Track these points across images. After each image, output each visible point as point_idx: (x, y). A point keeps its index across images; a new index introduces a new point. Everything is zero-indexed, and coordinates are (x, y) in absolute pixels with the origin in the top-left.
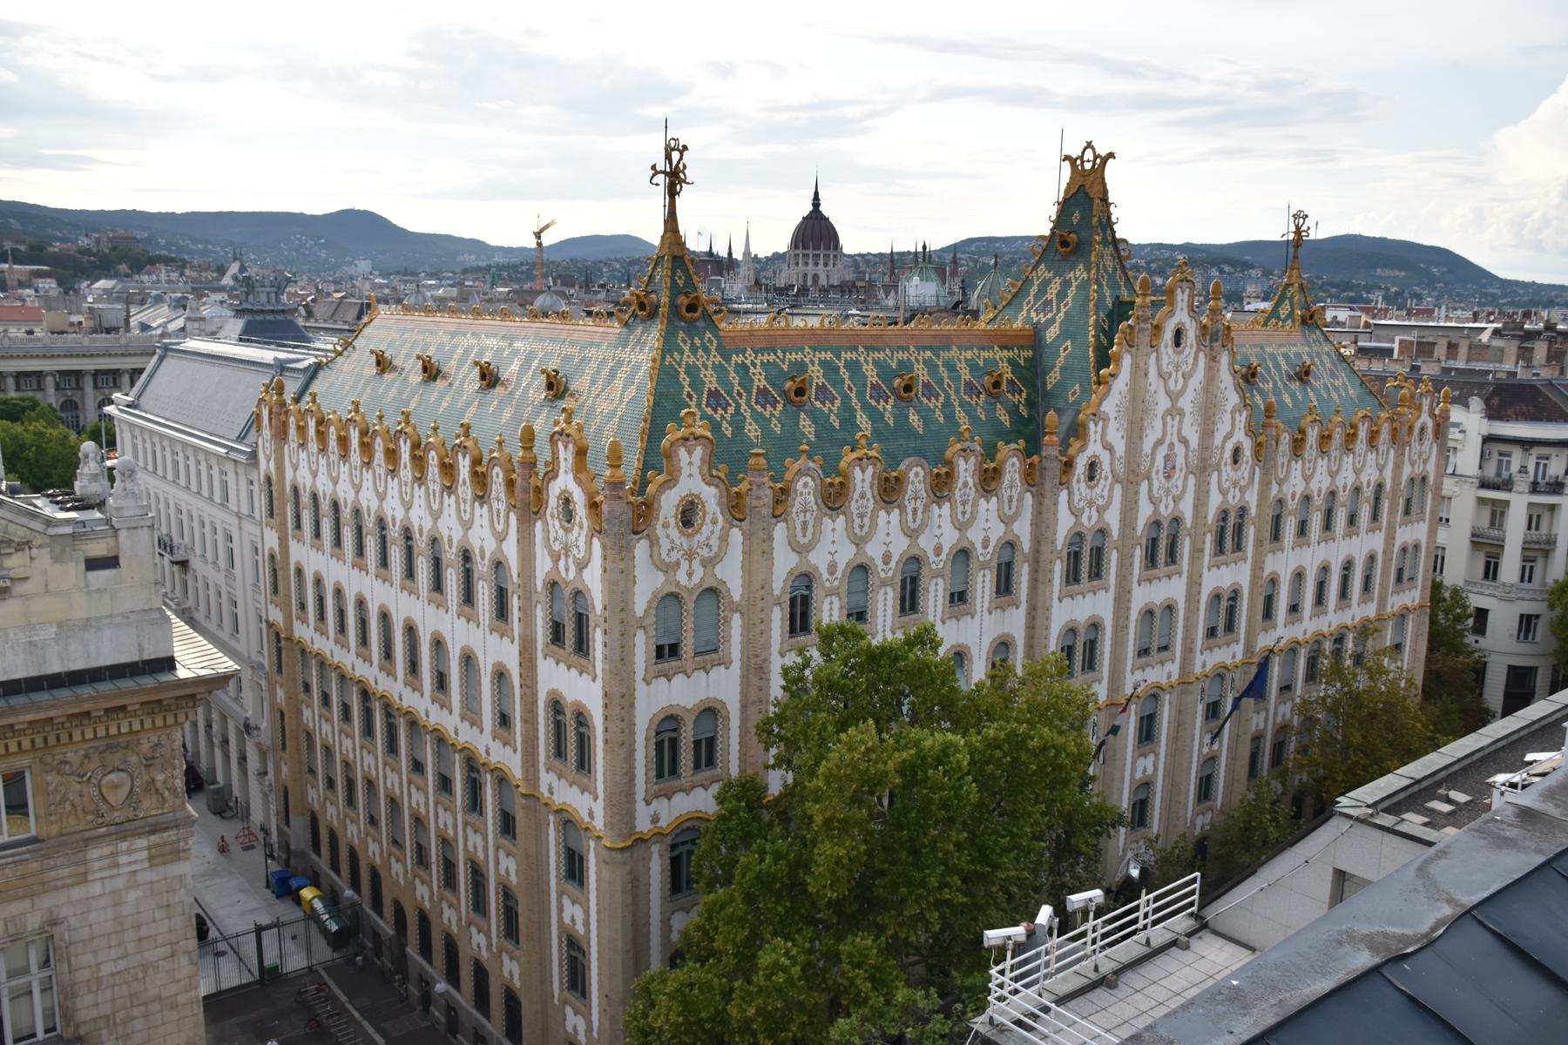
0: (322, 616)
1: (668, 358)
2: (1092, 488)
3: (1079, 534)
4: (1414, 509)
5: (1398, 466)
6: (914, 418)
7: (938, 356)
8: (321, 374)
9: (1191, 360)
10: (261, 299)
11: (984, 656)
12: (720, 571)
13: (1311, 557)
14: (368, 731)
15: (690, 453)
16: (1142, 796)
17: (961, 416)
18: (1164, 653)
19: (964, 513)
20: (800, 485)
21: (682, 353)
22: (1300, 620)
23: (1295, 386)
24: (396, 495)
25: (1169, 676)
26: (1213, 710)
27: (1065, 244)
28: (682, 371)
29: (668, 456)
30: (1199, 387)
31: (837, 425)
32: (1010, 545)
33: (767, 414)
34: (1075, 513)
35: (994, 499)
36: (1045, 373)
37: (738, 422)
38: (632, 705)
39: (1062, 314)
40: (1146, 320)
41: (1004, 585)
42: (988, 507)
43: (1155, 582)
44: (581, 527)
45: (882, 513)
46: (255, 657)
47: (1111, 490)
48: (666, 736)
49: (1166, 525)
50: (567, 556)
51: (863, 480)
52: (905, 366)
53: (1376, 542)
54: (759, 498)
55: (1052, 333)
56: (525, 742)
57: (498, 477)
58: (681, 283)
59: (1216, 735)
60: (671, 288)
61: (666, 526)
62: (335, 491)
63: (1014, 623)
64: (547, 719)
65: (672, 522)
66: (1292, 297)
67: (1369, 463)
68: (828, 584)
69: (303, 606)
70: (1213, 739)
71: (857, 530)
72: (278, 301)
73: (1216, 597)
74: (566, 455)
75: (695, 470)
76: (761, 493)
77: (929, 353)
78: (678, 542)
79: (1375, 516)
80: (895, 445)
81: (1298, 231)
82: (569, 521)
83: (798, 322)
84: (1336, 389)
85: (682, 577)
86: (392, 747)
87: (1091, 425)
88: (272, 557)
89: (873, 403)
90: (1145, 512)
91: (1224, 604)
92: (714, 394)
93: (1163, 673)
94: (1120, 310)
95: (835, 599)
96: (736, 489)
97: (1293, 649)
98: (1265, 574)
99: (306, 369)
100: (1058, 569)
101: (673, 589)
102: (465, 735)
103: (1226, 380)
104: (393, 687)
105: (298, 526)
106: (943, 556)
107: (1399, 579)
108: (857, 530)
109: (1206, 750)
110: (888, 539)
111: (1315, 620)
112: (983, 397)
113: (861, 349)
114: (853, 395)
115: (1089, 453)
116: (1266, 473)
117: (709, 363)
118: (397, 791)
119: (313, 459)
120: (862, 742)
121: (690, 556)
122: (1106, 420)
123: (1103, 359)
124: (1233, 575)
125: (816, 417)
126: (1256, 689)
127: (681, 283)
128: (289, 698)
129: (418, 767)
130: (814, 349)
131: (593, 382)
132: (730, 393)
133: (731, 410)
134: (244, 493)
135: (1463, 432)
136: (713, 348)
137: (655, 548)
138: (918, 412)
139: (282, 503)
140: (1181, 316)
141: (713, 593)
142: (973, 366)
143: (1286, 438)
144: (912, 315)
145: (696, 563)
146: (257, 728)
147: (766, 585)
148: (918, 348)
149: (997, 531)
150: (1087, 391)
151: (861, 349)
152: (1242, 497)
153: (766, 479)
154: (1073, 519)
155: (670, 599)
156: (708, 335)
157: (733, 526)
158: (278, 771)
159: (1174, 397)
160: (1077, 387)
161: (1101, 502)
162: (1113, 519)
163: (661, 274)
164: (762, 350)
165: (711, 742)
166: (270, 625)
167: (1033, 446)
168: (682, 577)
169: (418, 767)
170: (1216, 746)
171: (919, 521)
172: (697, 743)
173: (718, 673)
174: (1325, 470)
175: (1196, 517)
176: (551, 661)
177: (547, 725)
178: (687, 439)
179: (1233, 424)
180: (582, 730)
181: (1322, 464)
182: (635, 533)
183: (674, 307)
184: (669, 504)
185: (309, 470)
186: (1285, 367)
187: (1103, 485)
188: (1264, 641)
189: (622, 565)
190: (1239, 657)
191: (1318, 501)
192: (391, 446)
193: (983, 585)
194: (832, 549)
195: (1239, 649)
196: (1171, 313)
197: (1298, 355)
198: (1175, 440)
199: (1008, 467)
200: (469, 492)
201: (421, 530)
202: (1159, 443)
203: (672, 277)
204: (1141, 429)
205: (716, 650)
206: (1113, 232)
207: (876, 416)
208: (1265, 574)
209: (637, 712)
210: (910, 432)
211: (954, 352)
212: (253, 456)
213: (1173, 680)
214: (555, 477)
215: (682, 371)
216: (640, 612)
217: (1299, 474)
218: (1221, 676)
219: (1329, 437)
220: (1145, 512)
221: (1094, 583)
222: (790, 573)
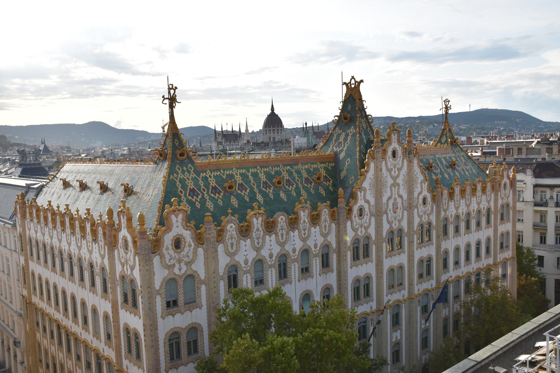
0: (42, 293)
1: (171, 176)
2: (361, 219)
3: (357, 239)
4: (505, 218)
5: (496, 200)
6: (282, 195)
7: (293, 168)
8: (45, 190)
9: (400, 163)
10: (31, 159)
11: (319, 294)
12: (194, 267)
13: (462, 241)
14: (60, 343)
15: (177, 217)
16: (397, 349)
17: (303, 192)
18: (401, 286)
19: (305, 234)
20: (228, 227)
21: (178, 174)
22: (460, 267)
23: (450, 170)
24: (65, 240)
25: (403, 296)
26: (425, 309)
27: (345, 118)
28: (178, 181)
29: (167, 219)
31: (248, 200)
32: (327, 246)
33: (216, 197)
34: (355, 230)
35: (318, 227)
36: (341, 171)
37: (203, 202)
38: (157, 329)
40: (378, 148)
41: (326, 264)
42: (316, 231)
43: (393, 257)
44: (131, 252)
45: (267, 237)
46: (19, 311)
47: (370, 219)
48: (174, 341)
49: (396, 232)
50: (127, 264)
51: (257, 223)
52: (278, 173)
53: (490, 232)
54: (209, 234)
55: (342, 155)
56: (116, 346)
57: (100, 230)
58: (177, 144)
59: (427, 320)
60: (175, 146)
61: (167, 249)
62: (44, 239)
63: (332, 279)
64: (124, 336)
65: (170, 247)
67: (483, 200)
68: (245, 269)
69: (35, 289)
70: (426, 321)
71: (256, 245)
72: (36, 160)
73: (421, 261)
74: (124, 221)
75: (179, 224)
76: (210, 232)
77: (288, 167)
78: (173, 255)
79: (488, 222)
80: (272, 208)
81: (447, 108)
82: (127, 249)
83: (252, 157)
84: (467, 170)
85: (176, 271)
86: (69, 350)
87: (359, 193)
88: (23, 268)
89: (264, 189)
90: (386, 227)
91: (425, 264)
92: (192, 191)
93: (401, 295)
94: (369, 144)
95: (248, 275)
96: (199, 231)
97: (458, 280)
98: (442, 249)
99: (37, 188)
100: (349, 255)
101: (173, 276)
102: (95, 344)
103: (417, 169)
104: (67, 322)
105: (32, 255)
106: (297, 253)
107: (502, 247)
108: (256, 245)
109: (423, 326)
110: (271, 247)
111: (466, 267)
112: (313, 184)
113: (258, 167)
114: (255, 187)
116: (438, 207)
117: (190, 177)
118: (72, 369)
119: (36, 226)
120: (243, 344)
121: (180, 261)
122: (365, 190)
123: (363, 166)
124: (429, 251)
125: (238, 197)
126: (443, 297)
127: (177, 144)
128: (30, 329)
129: (78, 358)
130: (237, 169)
131: (142, 188)
132: (199, 190)
133: (200, 197)
134: (12, 240)
135: (524, 184)
136: (192, 171)
137: (163, 259)
138: (284, 192)
139: (26, 246)
140: (395, 145)
141: (191, 277)
142: (308, 171)
143: (446, 192)
144: (298, 151)
145: (183, 264)
146: (20, 343)
147: (216, 271)
148: (284, 166)
149: (320, 240)
150: (357, 179)
151: (258, 167)
152: (429, 218)
153: (213, 226)
154: (354, 233)
155: (171, 282)
156: (190, 165)
157: (198, 247)
158: (28, 360)
159: (395, 178)
160: (353, 177)
161: (366, 225)
162: (372, 231)
163: (169, 141)
164: (214, 171)
165: (195, 342)
166: (23, 297)
167: (334, 204)
168: (176, 271)
169: (78, 358)
170: (427, 324)
171: (284, 239)
172: (189, 343)
173: (196, 311)
174: (464, 204)
175: (409, 227)
176: (124, 310)
177: (124, 339)
178: (175, 211)
179: (422, 188)
180: (137, 340)
181: (463, 202)
182: (153, 253)
183: (174, 154)
184: (168, 239)
185: (36, 231)
186: (445, 163)
187: (366, 218)
188: (444, 278)
189: (147, 268)
190: (434, 285)
191: (463, 217)
192: (62, 219)
193: (316, 264)
194: (246, 253)
195: (433, 282)
196: (390, 144)
197: (450, 157)
198: (397, 196)
199: (323, 213)
200: (91, 238)
201: (75, 254)
202: (390, 198)
203: (173, 142)
205: (195, 302)
206: (365, 112)
207: (265, 195)
208: (442, 249)
209: (159, 332)
210: (281, 201)
211: (300, 166)
212: (14, 226)
213: (405, 297)
214: (121, 230)
215: (178, 181)
216: (157, 288)
217: (453, 206)
218: (427, 295)
219: (465, 190)
220: (386, 227)
221: (366, 259)
222: (227, 265)
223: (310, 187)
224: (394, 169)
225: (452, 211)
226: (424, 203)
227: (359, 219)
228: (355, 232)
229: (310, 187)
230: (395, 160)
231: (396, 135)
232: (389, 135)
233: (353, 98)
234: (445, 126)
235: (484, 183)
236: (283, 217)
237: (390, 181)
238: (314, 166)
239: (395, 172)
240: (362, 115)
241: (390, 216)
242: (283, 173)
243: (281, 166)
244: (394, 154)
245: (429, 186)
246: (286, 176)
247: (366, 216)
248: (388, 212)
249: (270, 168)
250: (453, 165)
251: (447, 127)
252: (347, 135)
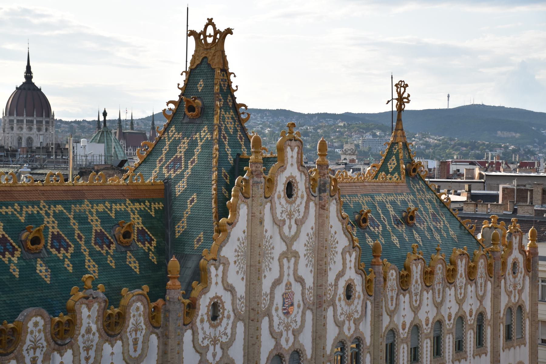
2: (215, 327)
5: (496, 297)
6: (41, 269)
7: (69, 210)
9: (302, 209)
17: (91, 264)
23: (402, 229)
27: (191, 109)
30: (311, 232)
35: (119, 343)
39: (189, 170)
40: (258, 175)
47: (234, 327)
55: (180, 187)
66: (397, 156)
67: (469, 294)
77: (60, 207)
81: (401, 100)
84: (438, 231)
87: (212, 269)
94: (240, 164)
103: (335, 224)
112: (113, 247)
115: (211, 294)
116: (377, 306)
122: (226, 264)
138: (46, 263)
140: (291, 170)
142: (104, 218)
143: (393, 275)
144: (83, 172)
148: (49, 203)
150: (209, 239)
152: (357, 329)
159: (289, 241)
160: (201, 235)
161: (224, 339)
167: (158, 291)
174: (430, 301)
179: (344, 264)
181: (427, 296)
186: (392, 213)
187: (226, 325)
191: (427, 329)
196: (283, 168)
197: (404, 202)
198: (292, 279)
199: (132, 311)
202: (277, 283)
204: (259, 271)
206: (234, 98)
210: (38, 282)
211: (86, 206)
217: (407, 305)
219: (432, 273)
223: (108, 253)
224: (287, 222)
225: (405, 316)
226: (348, 296)
227: (212, 326)
228: (201, 354)
229: (108, 253)
230: (291, 203)
231: (296, 149)
232: (281, 149)
233: (209, 63)
234: (395, 136)
235: (472, 258)
236: (39, 319)
237: (280, 247)
238: (118, 207)
239: (290, 228)
240: (226, 103)
241: (276, 321)
242: (46, 219)
243: (42, 203)
244: (290, 189)
245: (359, 260)
246: (53, 228)
247: (225, 321)
248: (274, 312)
249: (16, 206)
250: (408, 219)
251: (399, 138)
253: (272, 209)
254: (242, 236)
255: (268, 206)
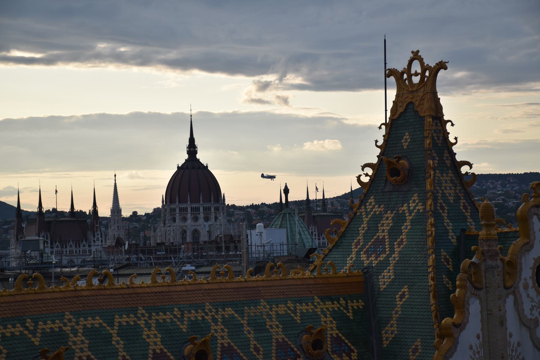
27: (394, 172)
39: (396, 255)
55: (386, 277)
77: (230, 311)
113: (141, 311)
123: (447, 306)
142: (287, 323)
151: (141, 311)
160: (418, 343)
243: (208, 306)
249: (176, 311)
252: (399, 219)
253: (517, 304)
254: (475, 342)
255: (510, 300)
